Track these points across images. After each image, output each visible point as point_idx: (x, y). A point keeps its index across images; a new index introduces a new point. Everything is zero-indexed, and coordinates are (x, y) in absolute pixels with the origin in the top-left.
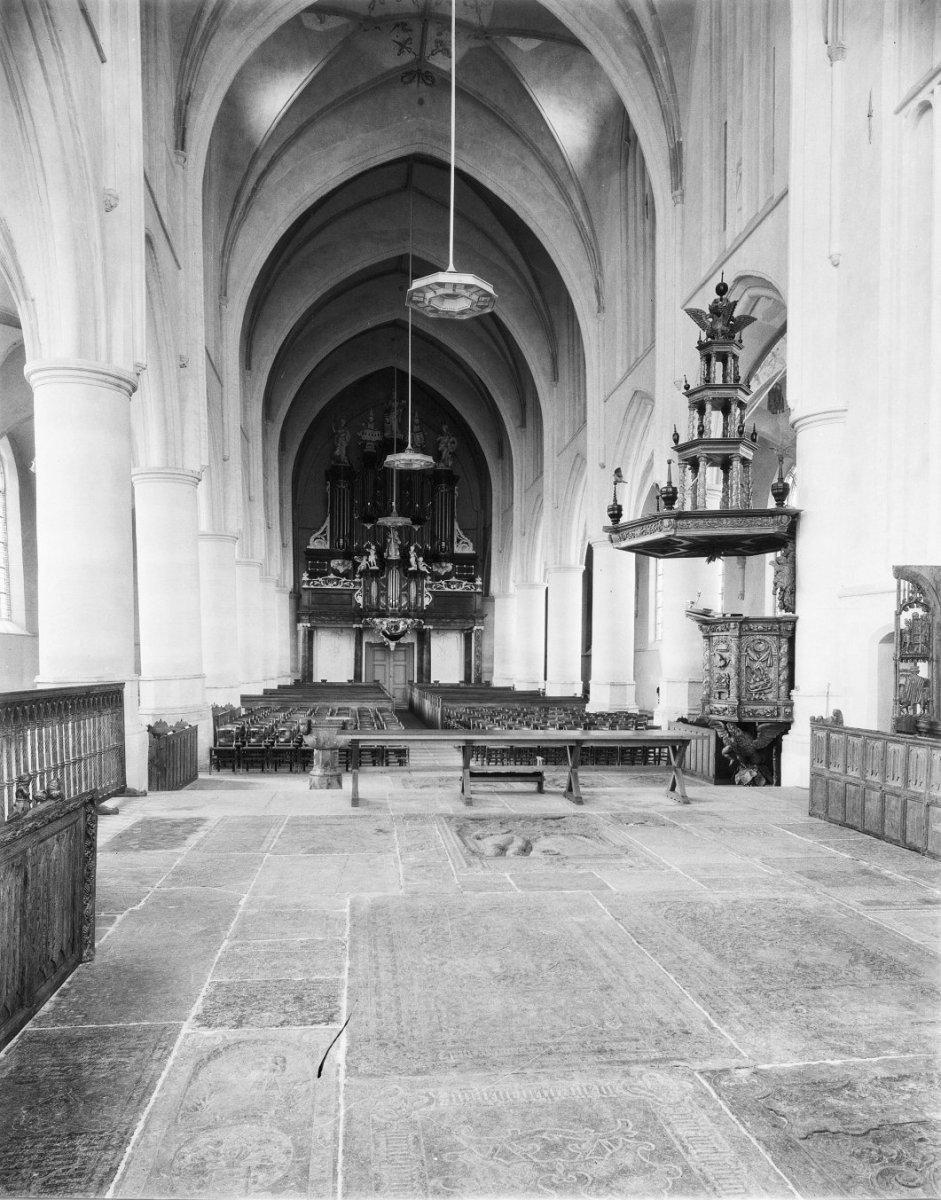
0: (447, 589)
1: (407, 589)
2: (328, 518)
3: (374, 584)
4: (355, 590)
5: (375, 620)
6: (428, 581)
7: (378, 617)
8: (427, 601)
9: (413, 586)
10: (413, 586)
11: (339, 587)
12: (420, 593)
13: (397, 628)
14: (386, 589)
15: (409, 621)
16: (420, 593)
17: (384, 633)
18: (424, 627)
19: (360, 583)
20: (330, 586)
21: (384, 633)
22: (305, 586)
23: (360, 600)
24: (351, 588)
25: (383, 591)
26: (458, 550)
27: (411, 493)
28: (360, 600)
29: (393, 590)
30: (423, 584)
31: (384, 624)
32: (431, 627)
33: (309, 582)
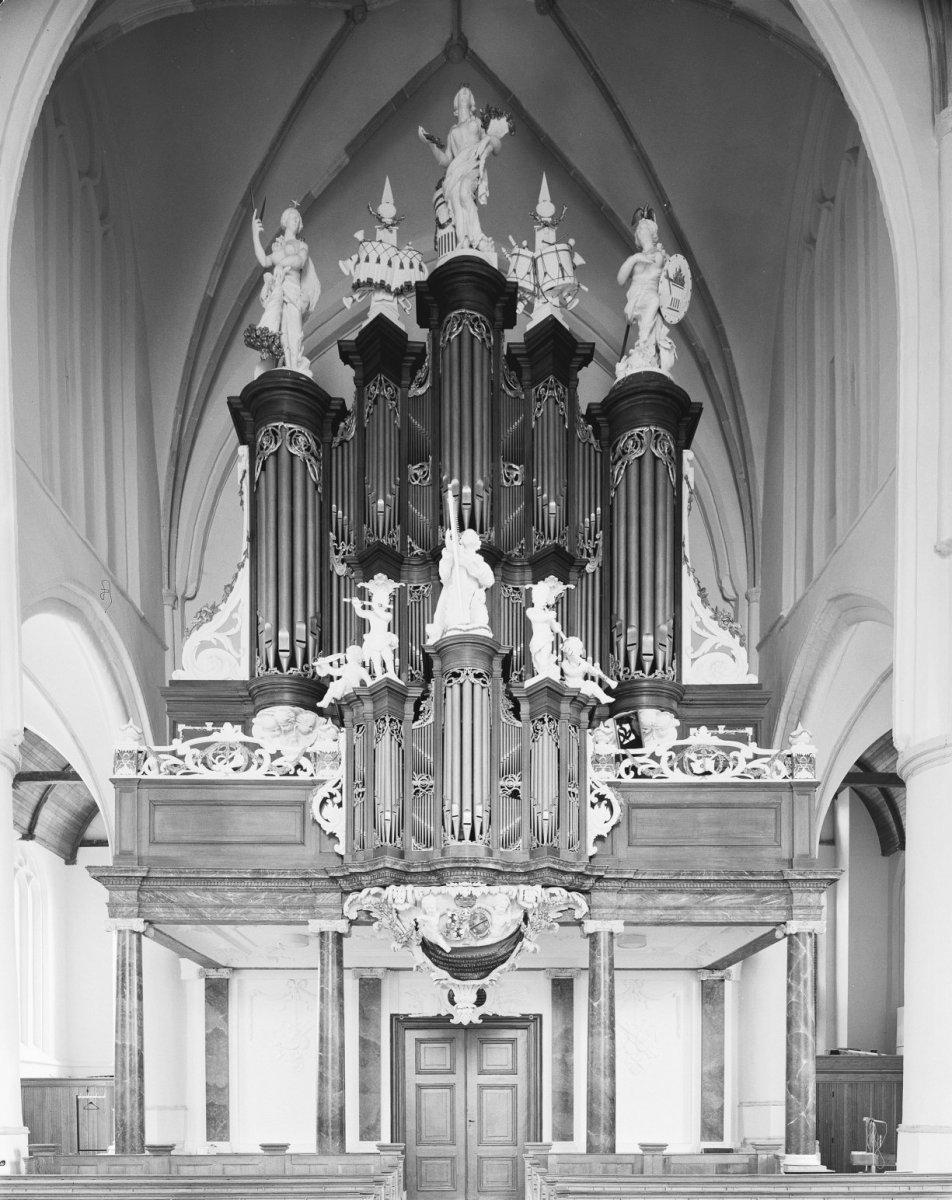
0: (677, 777)
1: (519, 765)
2: (245, 574)
3: (386, 748)
4: (315, 784)
5: (392, 891)
6: (604, 739)
7: (401, 878)
8: (598, 821)
9: (544, 749)
10: (544, 749)
11: (254, 774)
12: (570, 777)
13: (479, 925)
14: (437, 770)
15: (532, 894)
16: (570, 777)
17: (428, 947)
18: (590, 926)
19: (336, 757)
20: (221, 772)
21: (428, 947)
22: (127, 772)
23: (335, 819)
24: (302, 776)
25: (422, 767)
26: (692, 676)
27: (529, 472)
28: (335, 819)
29: (468, 789)
30: (582, 749)
31: (432, 910)
32: (618, 926)
33: (139, 758)
